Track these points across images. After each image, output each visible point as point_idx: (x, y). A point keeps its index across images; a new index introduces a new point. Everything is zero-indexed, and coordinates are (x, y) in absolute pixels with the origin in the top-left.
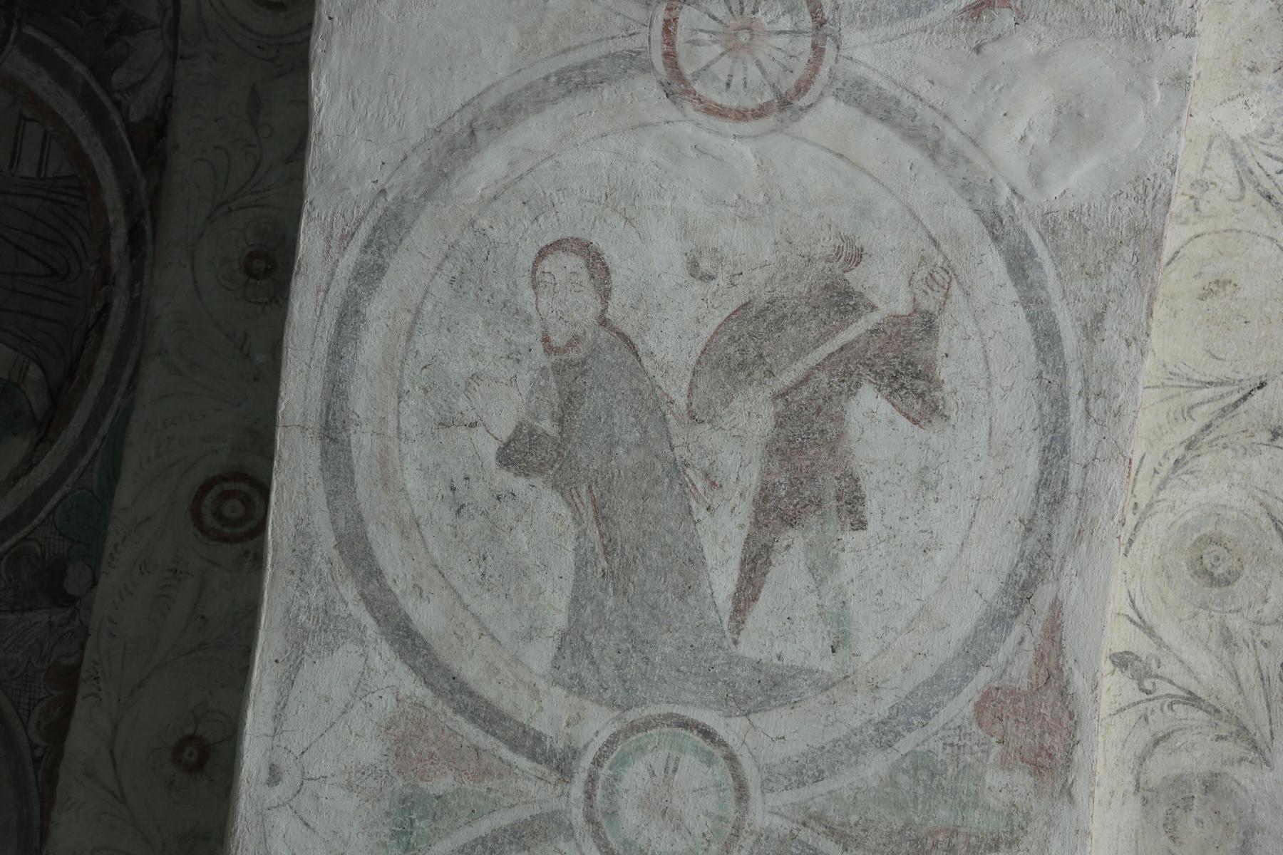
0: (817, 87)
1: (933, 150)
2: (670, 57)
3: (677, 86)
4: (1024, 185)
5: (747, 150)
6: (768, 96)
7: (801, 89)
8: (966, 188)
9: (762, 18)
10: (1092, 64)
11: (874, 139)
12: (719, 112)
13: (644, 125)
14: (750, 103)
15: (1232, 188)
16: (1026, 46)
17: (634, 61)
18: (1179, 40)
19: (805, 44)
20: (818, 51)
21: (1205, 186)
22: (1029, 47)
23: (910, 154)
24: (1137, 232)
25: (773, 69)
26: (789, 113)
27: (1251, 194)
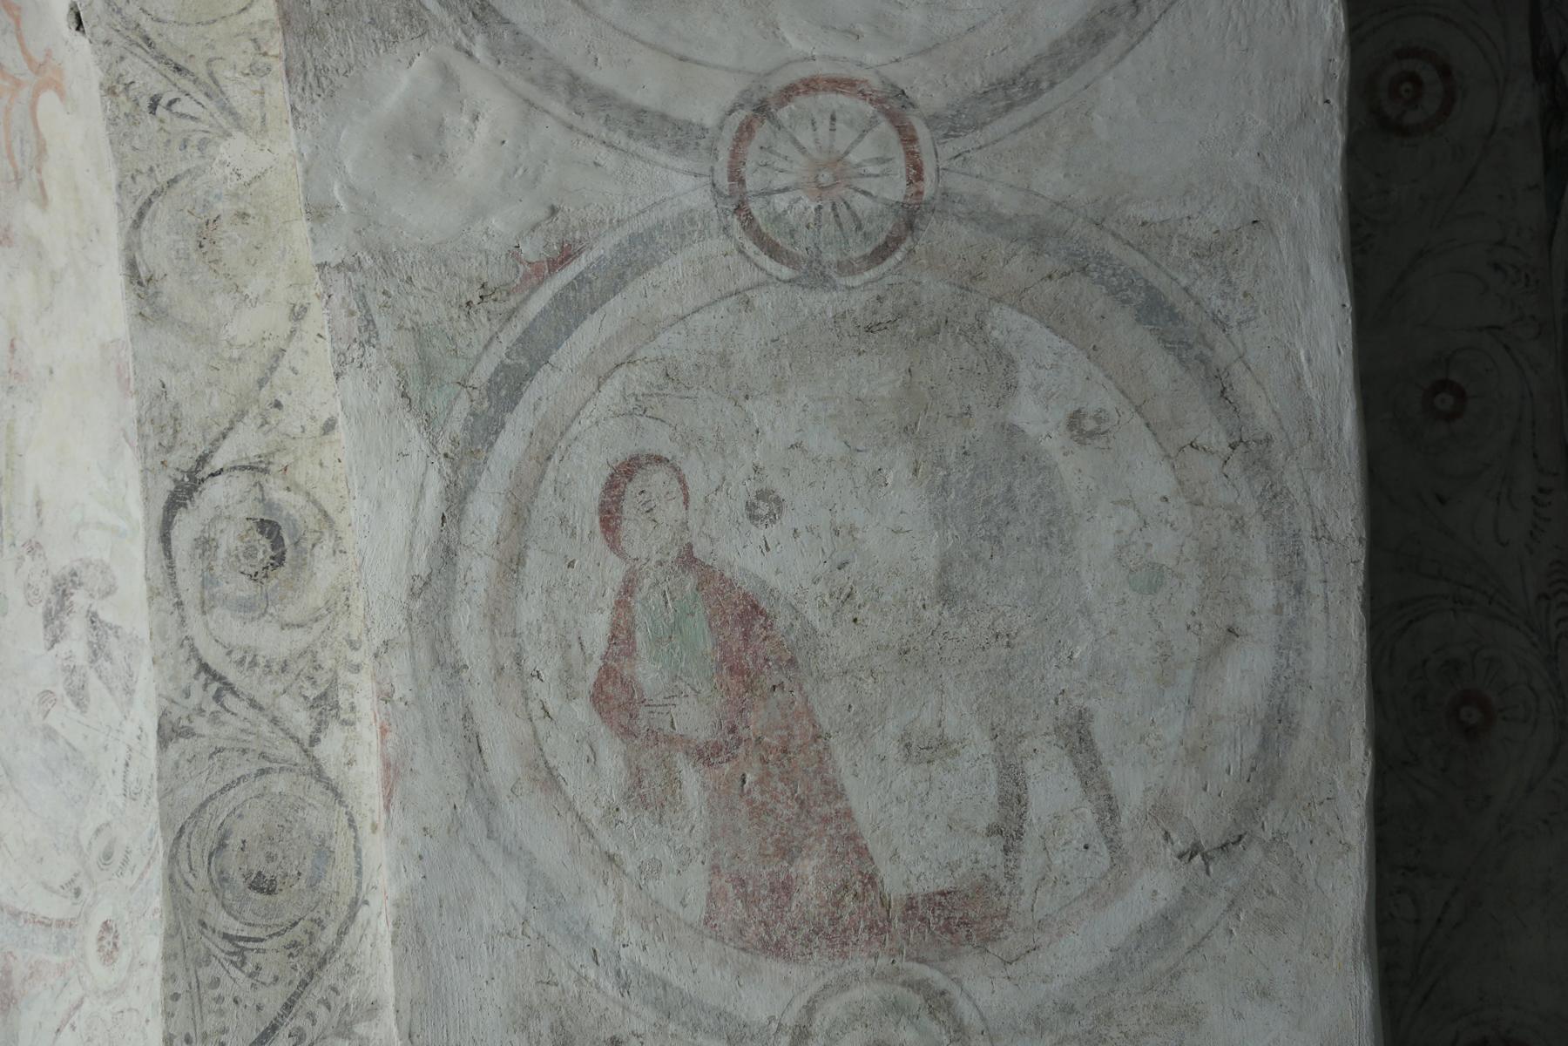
0: (728, 135)
1: (575, 86)
2: (908, 138)
3: (894, 106)
4: (459, 64)
5: (796, 45)
6: (783, 114)
7: (746, 130)
8: (526, 48)
9: (808, 203)
10: (421, 216)
11: (648, 85)
12: (838, 84)
13: (925, 51)
14: (803, 101)
15: (224, 73)
16: (502, 224)
17: (950, 125)
18: (333, 258)
19: (753, 181)
20: (736, 177)
21: (254, 71)
22: (496, 223)
23: (604, 76)
24: (313, 31)
25: (784, 147)
26: (755, 99)
27: (200, 69)
